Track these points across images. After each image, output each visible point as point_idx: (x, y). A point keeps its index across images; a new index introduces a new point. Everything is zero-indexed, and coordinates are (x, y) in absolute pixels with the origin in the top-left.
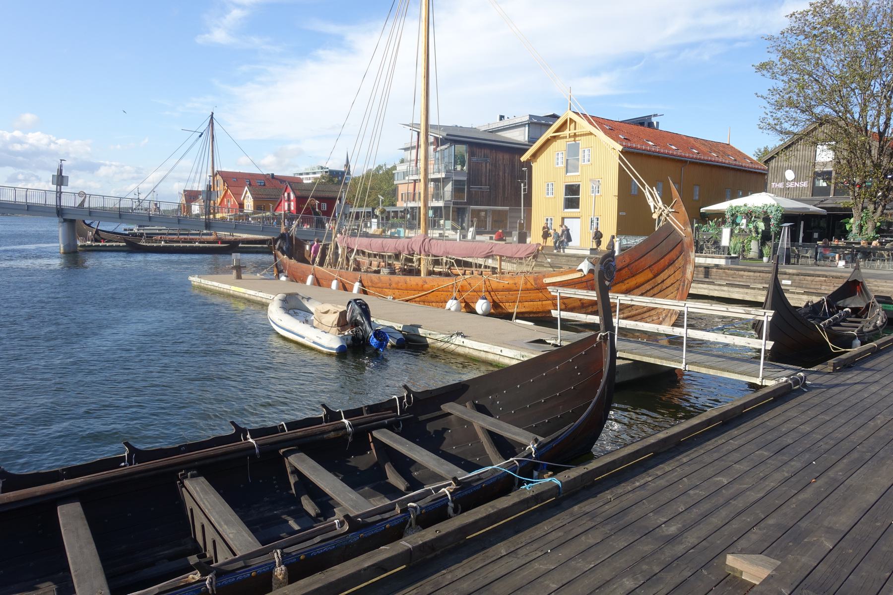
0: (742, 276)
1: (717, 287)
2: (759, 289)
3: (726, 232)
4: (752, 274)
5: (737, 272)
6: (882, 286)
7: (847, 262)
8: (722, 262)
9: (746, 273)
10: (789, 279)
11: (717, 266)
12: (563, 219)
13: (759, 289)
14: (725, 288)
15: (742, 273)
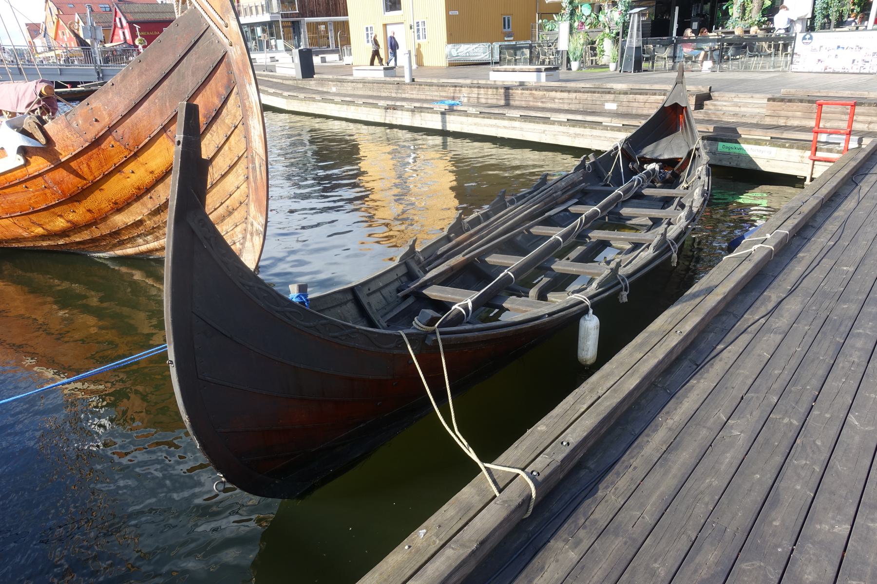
0: (553, 99)
1: (506, 123)
2: (560, 123)
3: (563, 27)
4: (565, 95)
5: (547, 94)
6: (746, 105)
7: (714, 62)
8: (530, 78)
9: (559, 95)
10: (614, 101)
11: (522, 84)
12: (385, 26)
13: (560, 123)
14: (517, 124)
15: (553, 94)
